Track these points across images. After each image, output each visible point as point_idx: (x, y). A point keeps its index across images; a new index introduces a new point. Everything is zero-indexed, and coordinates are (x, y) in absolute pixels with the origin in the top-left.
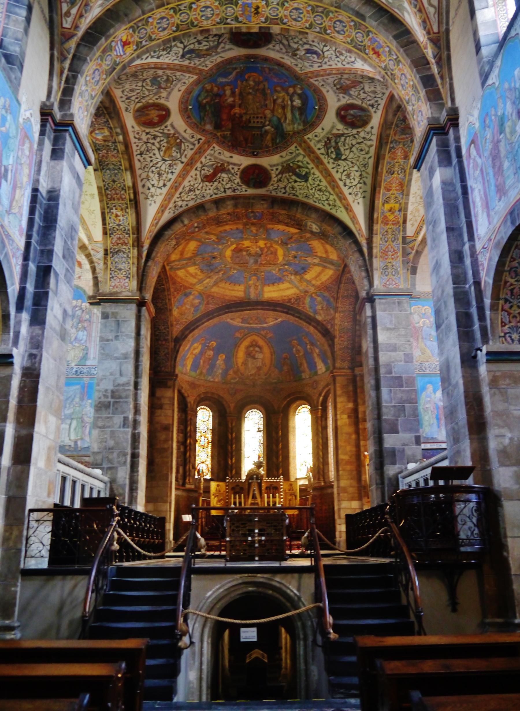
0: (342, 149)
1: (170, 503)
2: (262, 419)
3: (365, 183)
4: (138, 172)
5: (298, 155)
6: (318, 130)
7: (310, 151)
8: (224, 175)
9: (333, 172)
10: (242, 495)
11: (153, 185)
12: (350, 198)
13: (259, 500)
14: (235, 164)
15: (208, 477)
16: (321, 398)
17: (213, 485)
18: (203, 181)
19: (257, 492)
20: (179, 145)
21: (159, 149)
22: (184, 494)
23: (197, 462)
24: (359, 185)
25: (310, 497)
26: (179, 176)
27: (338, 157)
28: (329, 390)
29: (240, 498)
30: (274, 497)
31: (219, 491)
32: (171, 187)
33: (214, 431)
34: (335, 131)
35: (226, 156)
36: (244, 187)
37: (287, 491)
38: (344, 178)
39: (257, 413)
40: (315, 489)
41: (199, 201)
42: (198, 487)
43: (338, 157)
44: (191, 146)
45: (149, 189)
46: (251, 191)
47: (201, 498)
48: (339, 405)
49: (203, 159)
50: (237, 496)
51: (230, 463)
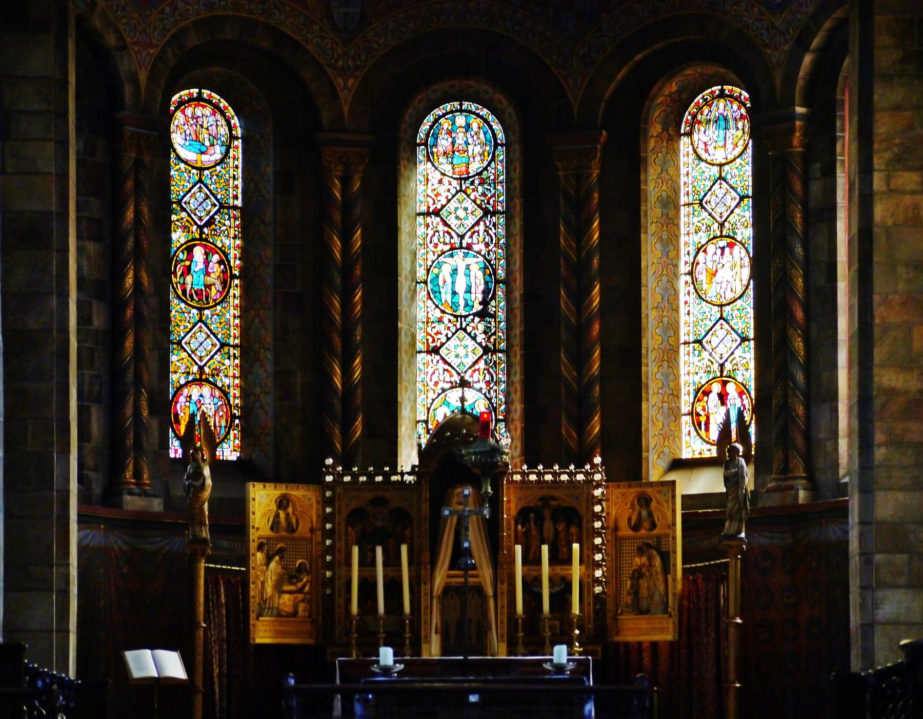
1: (65, 593)
2: (501, 154)
10: (404, 549)
13: (486, 574)
15: (229, 452)
16: (808, 59)
17: (262, 499)
19: (474, 540)
22: (118, 542)
23: (177, 378)
25: (735, 565)
28: (842, 24)
29: (392, 561)
30: (560, 558)
31: (291, 529)
33: (250, 219)
37: (625, 531)
39: (475, 123)
40: (760, 520)
42: (183, 511)
47: (203, 565)
48: (883, 126)
50: (379, 550)
51: (338, 381)
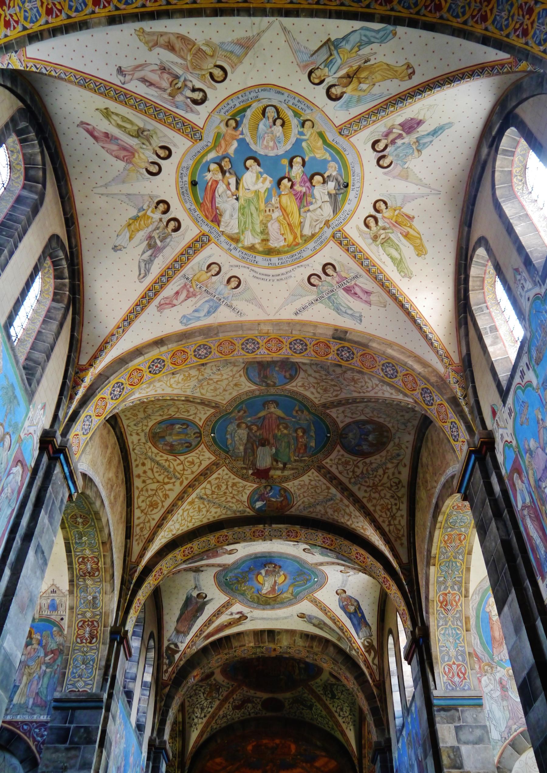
0: (336, 692)
3: (354, 715)
4: (187, 708)
5: (305, 693)
6: (318, 680)
7: (312, 692)
8: (250, 705)
9: (331, 706)
11: (197, 717)
12: (344, 726)
14: (258, 698)
18: (233, 709)
20: (218, 690)
21: (204, 693)
24: (350, 717)
26: (216, 709)
27: (333, 697)
32: (210, 717)
34: (329, 682)
35: (252, 693)
36: (264, 712)
38: (338, 710)
41: (229, 723)
43: (333, 697)
44: (226, 689)
45: (193, 719)
46: (269, 714)
49: (235, 696)
